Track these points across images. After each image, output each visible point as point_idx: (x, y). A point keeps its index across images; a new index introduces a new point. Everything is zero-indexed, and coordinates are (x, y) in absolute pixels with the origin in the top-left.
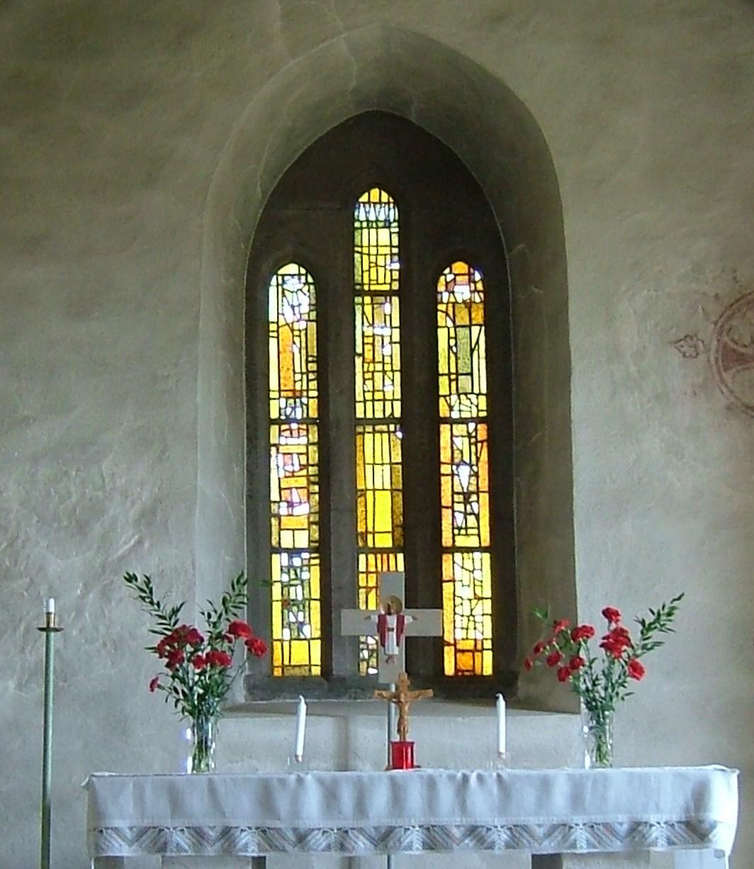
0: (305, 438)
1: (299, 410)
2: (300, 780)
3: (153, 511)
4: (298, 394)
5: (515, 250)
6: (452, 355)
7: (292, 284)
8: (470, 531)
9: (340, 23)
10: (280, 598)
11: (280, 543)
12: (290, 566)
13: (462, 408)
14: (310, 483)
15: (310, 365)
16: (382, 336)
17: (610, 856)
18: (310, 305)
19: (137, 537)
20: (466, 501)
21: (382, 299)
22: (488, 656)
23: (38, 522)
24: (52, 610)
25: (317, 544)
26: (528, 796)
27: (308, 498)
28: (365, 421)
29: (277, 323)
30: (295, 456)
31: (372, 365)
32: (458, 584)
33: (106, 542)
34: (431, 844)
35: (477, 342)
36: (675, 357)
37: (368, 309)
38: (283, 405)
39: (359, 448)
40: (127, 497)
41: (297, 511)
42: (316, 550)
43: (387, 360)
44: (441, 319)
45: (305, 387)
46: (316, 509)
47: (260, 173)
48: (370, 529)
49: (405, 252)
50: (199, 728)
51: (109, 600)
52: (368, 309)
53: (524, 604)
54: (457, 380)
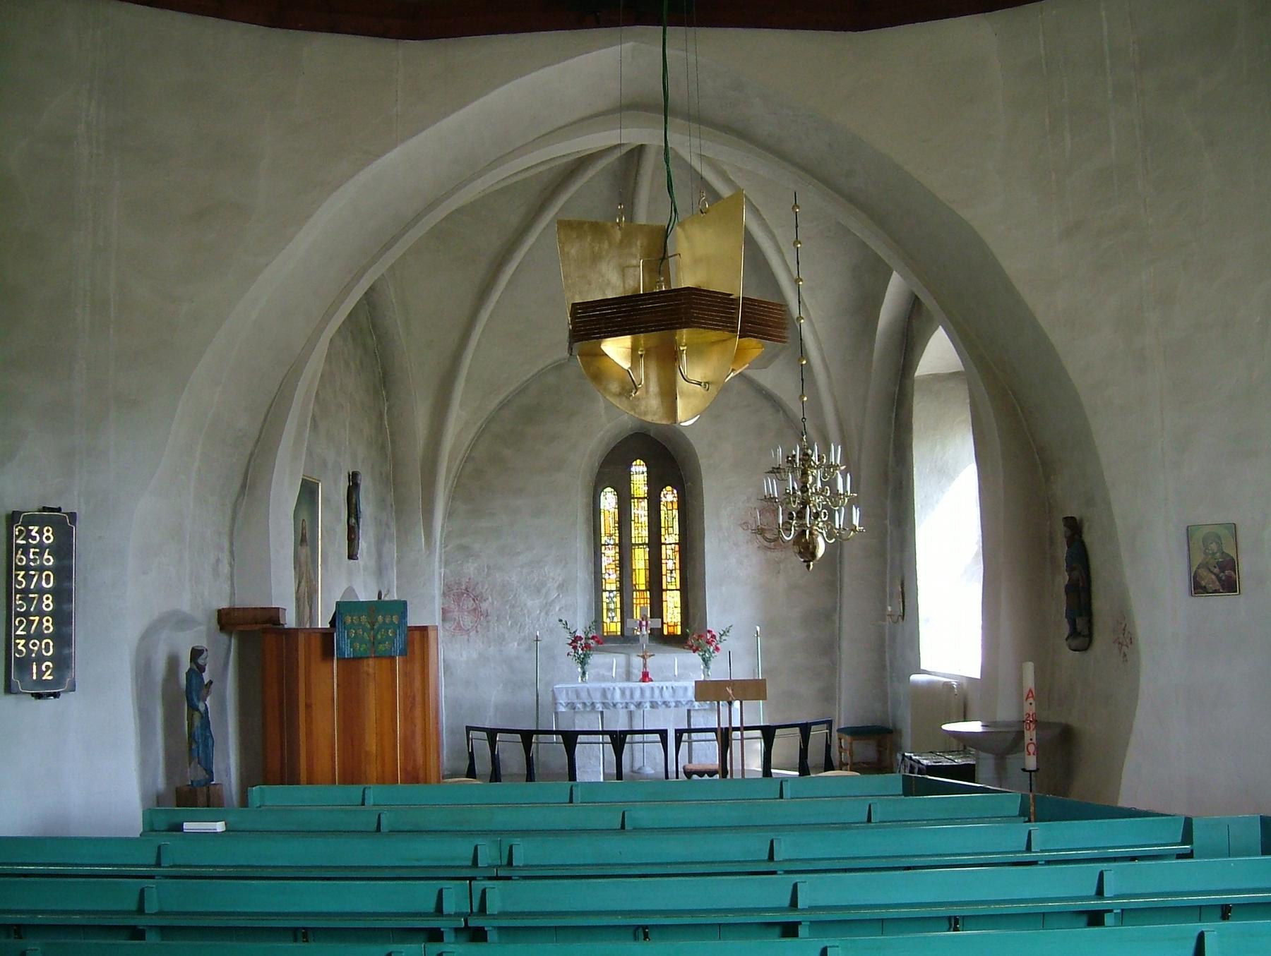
2: (614, 689)
12: (610, 597)
17: (705, 710)
20: (671, 573)
22: (679, 628)
24: (538, 634)
26: (681, 693)
28: (636, 544)
34: (652, 707)
36: (740, 530)
37: (636, 504)
42: (618, 591)
44: (662, 507)
46: (618, 576)
50: (582, 668)
52: (636, 504)
53: (691, 611)
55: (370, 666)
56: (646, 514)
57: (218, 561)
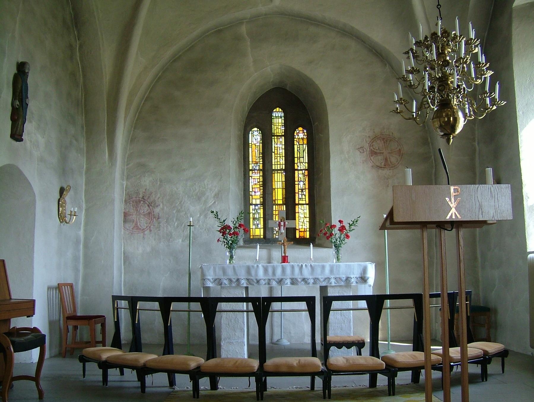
0: (259, 175)
1: (257, 167)
2: (258, 266)
3: (218, 194)
4: (257, 163)
5: (315, 124)
6: (298, 152)
7: (255, 133)
8: (303, 199)
9: (268, 64)
10: (252, 217)
11: (252, 203)
12: (255, 209)
13: (301, 166)
14: (260, 186)
15: (260, 155)
16: (280, 147)
17: (340, 286)
18: (260, 139)
19: (214, 201)
20: (302, 191)
21: (279, 137)
22: (308, 233)
23: (187, 197)
24: (191, 220)
25: (262, 203)
26: (319, 270)
27: (260, 191)
28: (275, 170)
29: (252, 144)
30: (256, 179)
31: (277, 155)
32: (300, 214)
33: (205, 202)
34: (293, 283)
35: (305, 149)
36: (358, 153)
37: (276, 140)
38: (253, 166)
39: (273, 177)
40: (211, 190)
41: (257, 194)
42: (262, 204)
43: (281, 154)
45: (259, 161)
46: (262, 193)
47: (247, 104)
48: (276, 199)
49: (286, 125)
50: (231, 252)
51: (206, 218)
52: (276, 140)
54: (300, 159)
56: (283, 147)
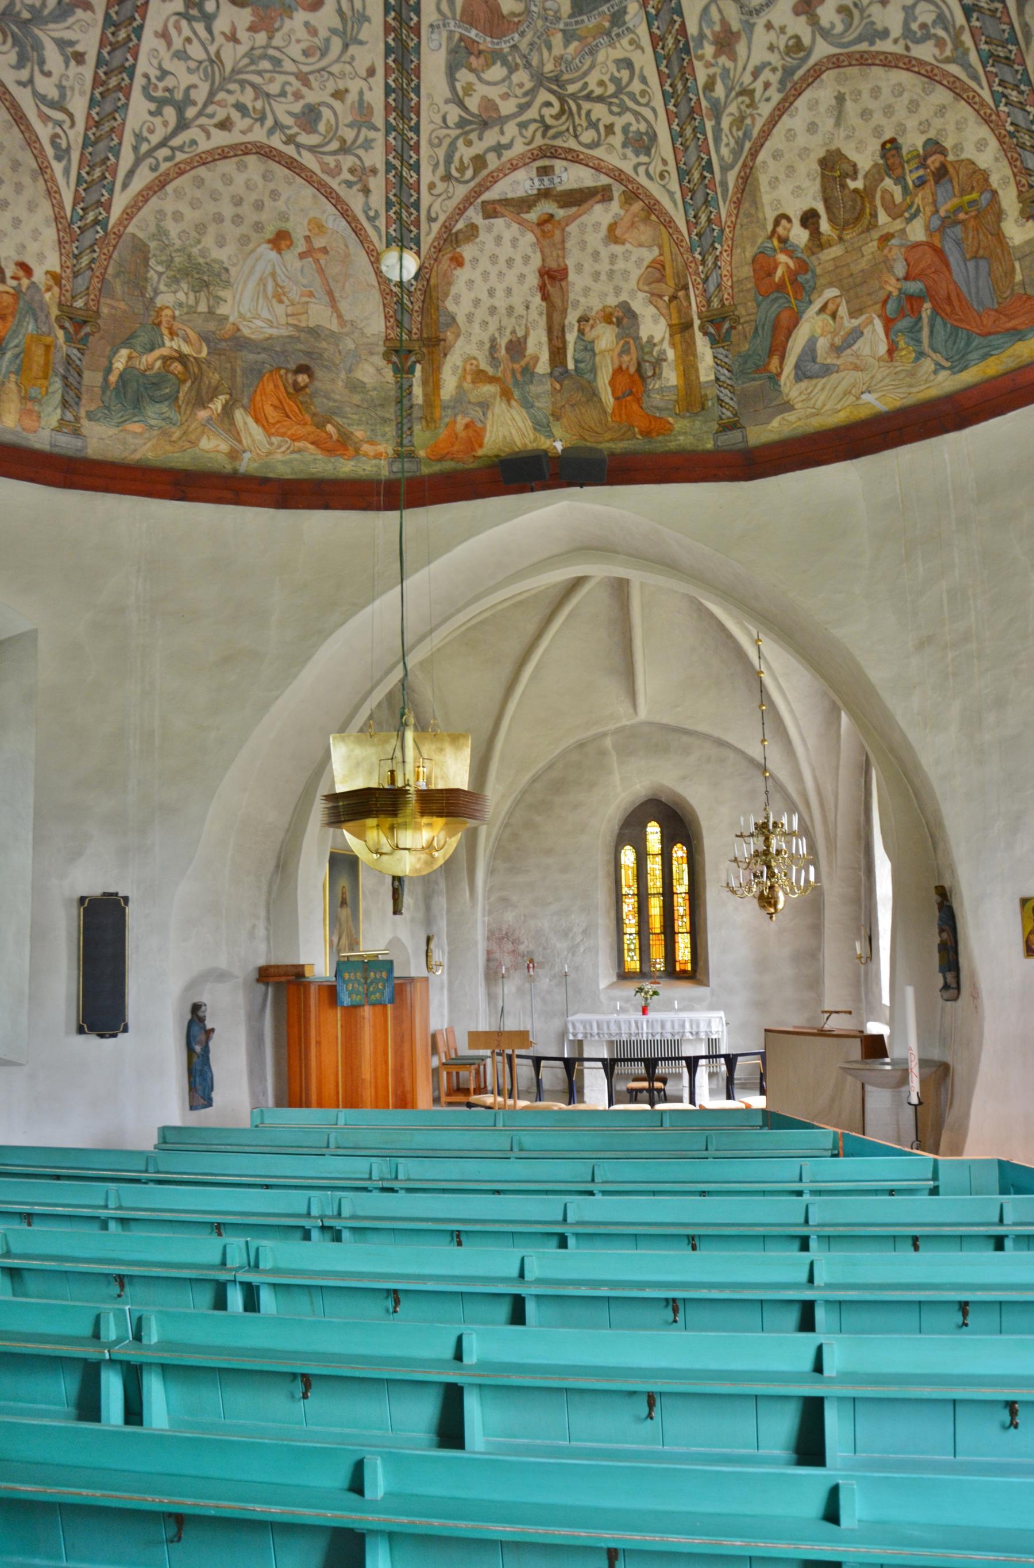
33: (573, 938)
55: (367, 1011)
57: (254, 926)
